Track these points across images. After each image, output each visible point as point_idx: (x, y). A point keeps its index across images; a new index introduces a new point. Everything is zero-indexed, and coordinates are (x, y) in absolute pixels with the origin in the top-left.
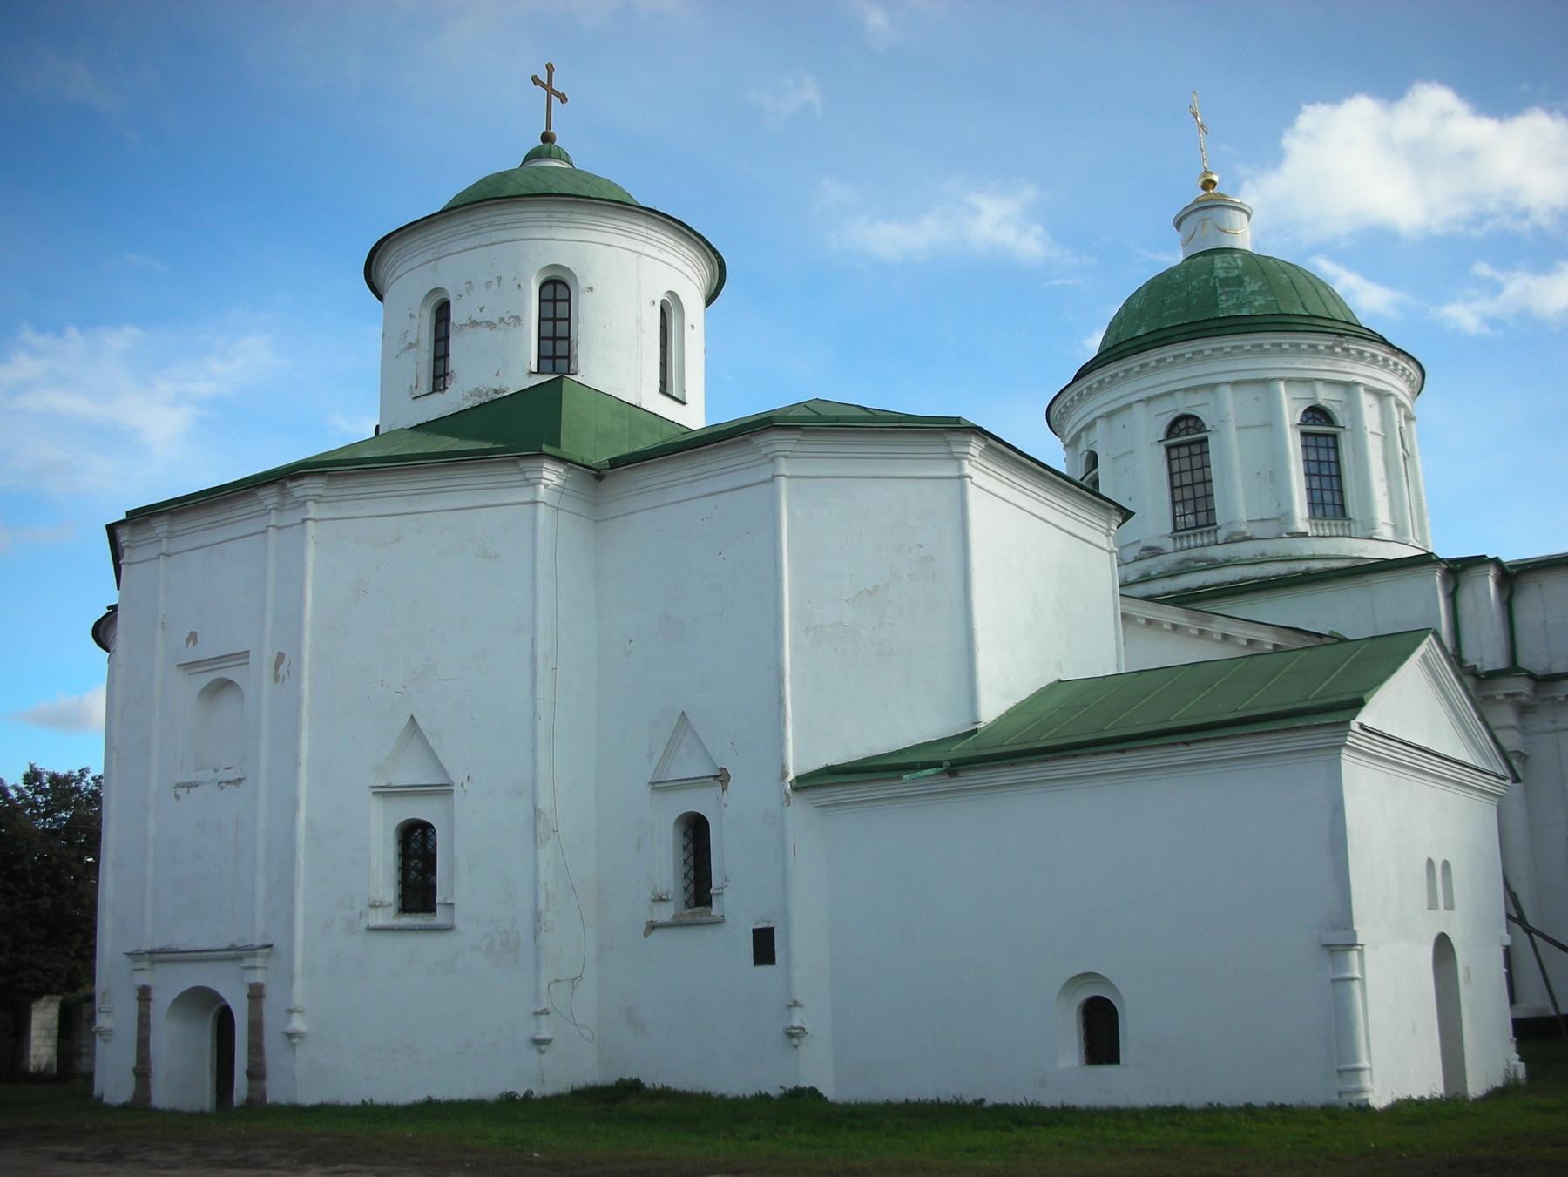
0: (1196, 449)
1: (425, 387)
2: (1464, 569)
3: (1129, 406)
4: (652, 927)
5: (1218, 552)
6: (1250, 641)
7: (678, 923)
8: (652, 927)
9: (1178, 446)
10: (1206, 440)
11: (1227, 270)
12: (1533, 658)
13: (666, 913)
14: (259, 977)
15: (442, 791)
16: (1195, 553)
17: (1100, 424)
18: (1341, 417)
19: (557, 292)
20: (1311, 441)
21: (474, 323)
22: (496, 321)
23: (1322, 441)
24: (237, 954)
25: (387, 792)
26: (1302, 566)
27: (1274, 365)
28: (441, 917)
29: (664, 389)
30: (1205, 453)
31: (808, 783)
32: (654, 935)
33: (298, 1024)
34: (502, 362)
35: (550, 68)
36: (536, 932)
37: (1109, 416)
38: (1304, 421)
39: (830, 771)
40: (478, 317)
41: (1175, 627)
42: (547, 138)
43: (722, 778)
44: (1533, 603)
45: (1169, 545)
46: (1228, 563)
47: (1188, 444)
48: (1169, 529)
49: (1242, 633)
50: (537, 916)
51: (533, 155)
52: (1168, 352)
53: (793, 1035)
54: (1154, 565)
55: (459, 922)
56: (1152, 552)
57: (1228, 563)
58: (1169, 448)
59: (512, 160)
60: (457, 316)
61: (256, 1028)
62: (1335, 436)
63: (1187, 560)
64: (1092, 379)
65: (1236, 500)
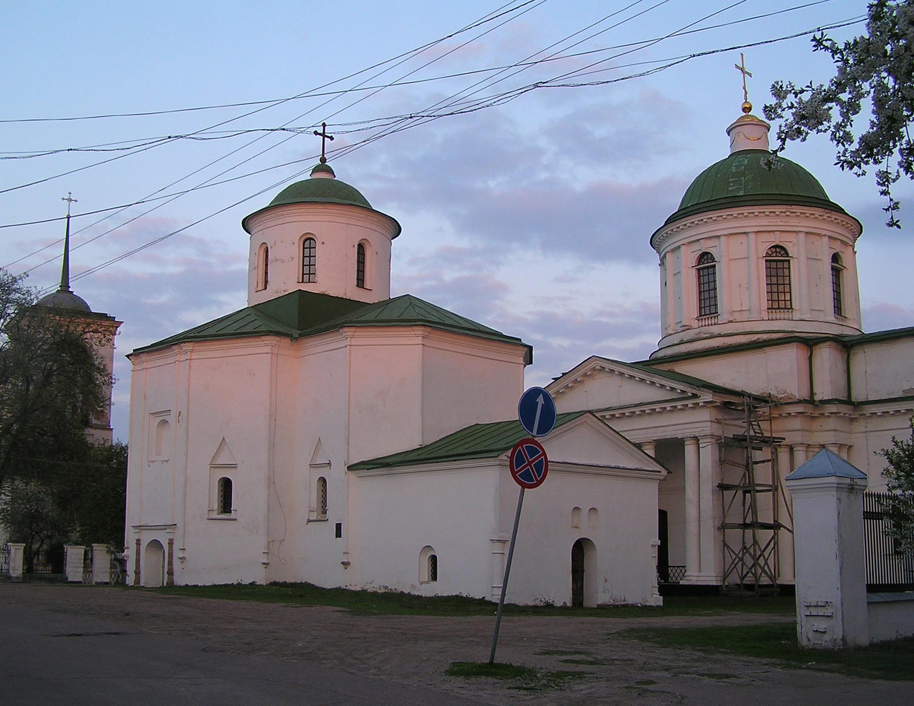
0: (711, 271)
1: (261, 287)
2: (815, 344)
3: (679, 247)
5: (715, 330)
6: (672, 389)
9: (703, 268)
10: (715, 266)
11: (737, 167)
12: (858, 395)
13: (314, 516)
15: (234, 466)
20: (774, 265)
21: (276, 260)
23: (780, 265)
24: (165, 527)
25: (214, 466)
26: (754, 337)
28: (233, 515)
29: (361, 282)
34: (285, 281)
35: (324, 125)
37: (673, 251)
38: (768, 255)
39: (363, 463)
41: (642, 380)
42: (323, 160)
44: (863, 360)
45: (695, 324)
46: (720, 336)
47: (708, 268)
48: (696, 314)
49: (669, 383)
51: (316, 170)
52: (704, 216)
53: (346, 564)
54: (690, 334)
56: (687, 328)
57: (720, 336)
58: (699, 270)
61: (171, 555)
62: (789, 261)
63: (700, 333)
64: (673, 226)
65: (726, 300)
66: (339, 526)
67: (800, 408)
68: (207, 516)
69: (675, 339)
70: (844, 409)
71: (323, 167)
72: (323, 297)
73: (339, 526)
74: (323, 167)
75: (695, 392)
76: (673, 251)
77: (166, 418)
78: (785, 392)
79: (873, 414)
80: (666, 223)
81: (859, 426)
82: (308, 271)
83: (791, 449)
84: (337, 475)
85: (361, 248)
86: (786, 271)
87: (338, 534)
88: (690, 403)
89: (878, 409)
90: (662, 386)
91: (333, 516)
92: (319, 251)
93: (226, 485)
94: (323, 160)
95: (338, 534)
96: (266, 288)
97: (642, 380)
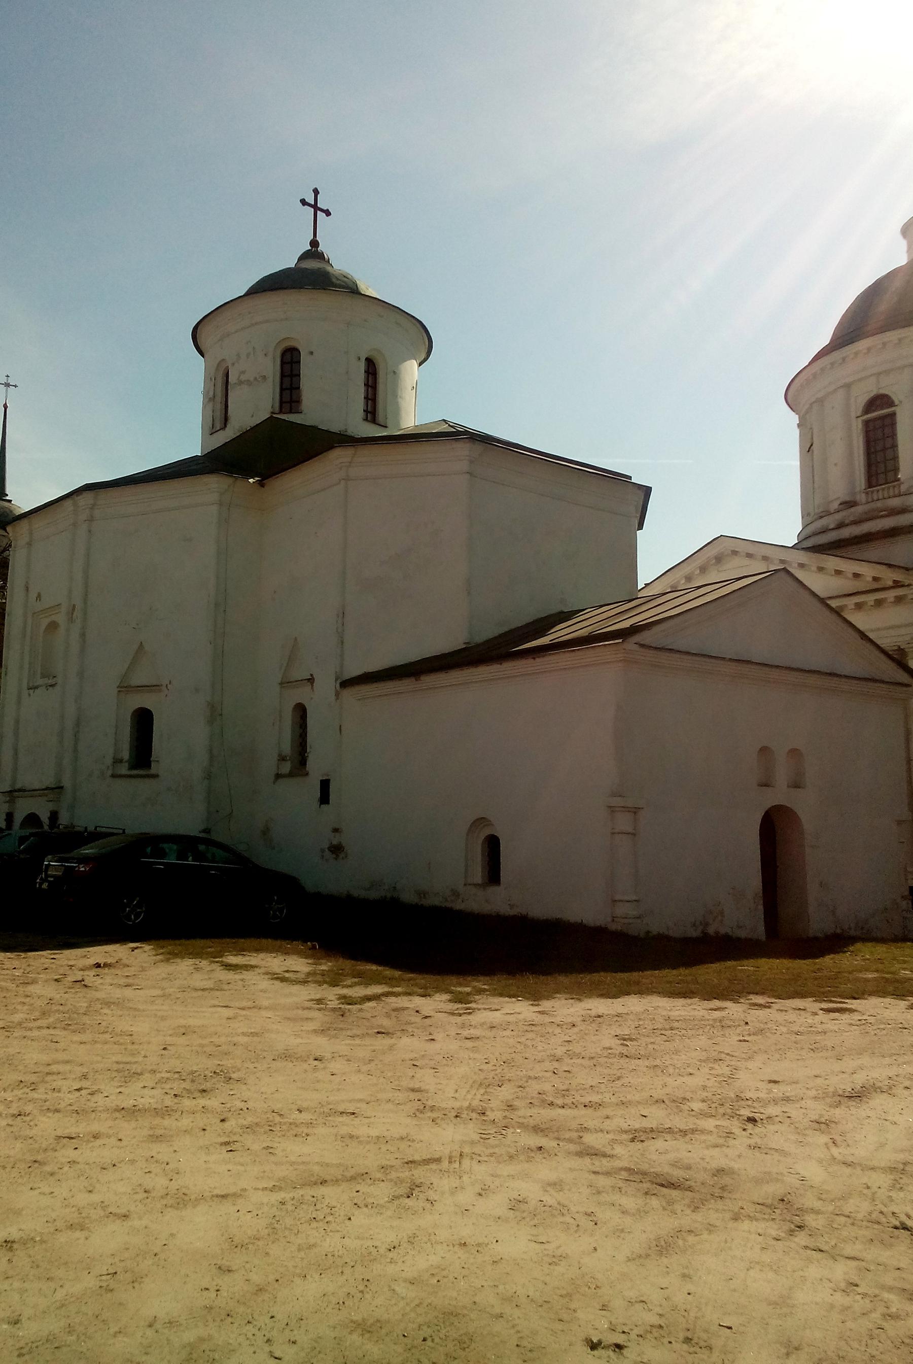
4: (278, 776)
5: (895, 502)
7: (291, 775)
10: (893, 415)
16: (879, 504)
21: (240, 383)
22: (252, 379)
29: (371, 414)
30: (893, 424)
31: (346, 684)
32: (280, 781)
40: (243, 378)
42: (314, 243)
43: (311, 680)
45: (862, 498)
51: (305, 256)
58: (867, 423)
59: (290, 262)
63: (873, 510)
66: (325, 785)
68: (110, 772)
69: (830, 521)
71: (314, 252)
73: (325, 785)
74: (314, 252)
77: (53, 618)
84: (321, 700)
87: (325, 798)
91: (317, 765)
93: (143, 721)
94: (314, 243)
95: (325, 798)
96: (225, 426)
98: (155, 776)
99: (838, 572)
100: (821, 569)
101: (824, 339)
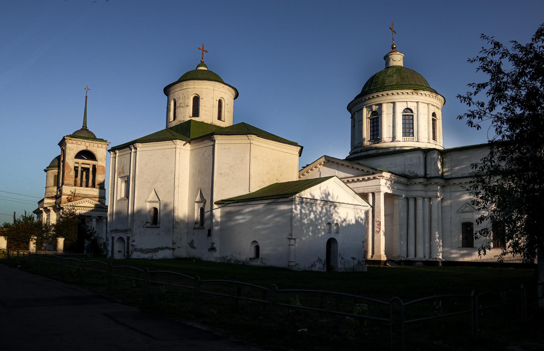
4: (195, 228)
6: (362, 170)
8: (195, 228)
9: (373, 119)
14: (129, 235)
17: (356, 113)
18: (415, 111)
19: (196, 100)
21: (180, 107)
27: (395, 98)
29: (219, 118)
32: (195, 230)
33: (134, 243)
36: (173, 228)
37: (358, 111)
40: (181, 105)
50: (173, 226)
55: (161, 227)
60: (178, 105)
62: (413, 115)
67: (421, 180)
70: (441, 181)
72: (202, 123)
75: (374, 171)
76: (358, 111)
78: (413, 173)
79: (454, 184)
80: (356, 98)
81: (447, 189)
82: (196, 112)
83: (415, 199)
85: (220, 102)
86: (411, 121)
88: (371, 177)
89: (457, 181)
90: (357, 169)
92: (202, 103)
97: (348, 166)
98: (159, 227)
99: (357, 169)
100: (353, 168)
101: (359, 92)
